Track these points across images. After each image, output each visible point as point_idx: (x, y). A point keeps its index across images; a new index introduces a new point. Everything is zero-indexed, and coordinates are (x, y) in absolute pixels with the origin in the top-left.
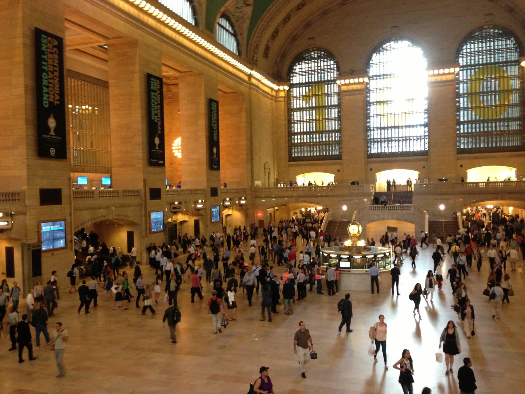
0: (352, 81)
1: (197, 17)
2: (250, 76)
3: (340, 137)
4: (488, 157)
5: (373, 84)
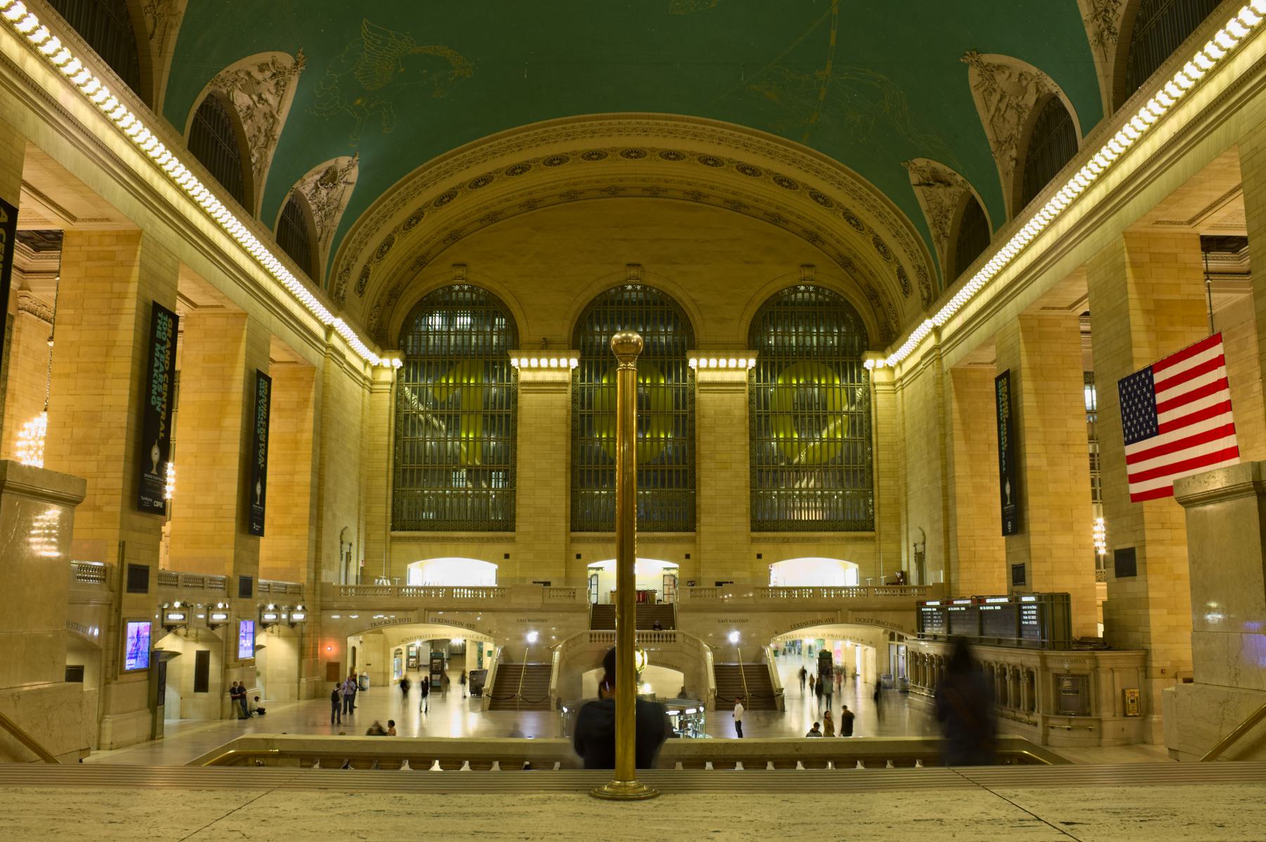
2: (329, 330)
4: (808, 540)
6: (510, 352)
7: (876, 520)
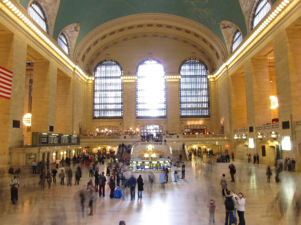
0: (129, 78)
1: (48, 30)
2: (74, 69)
3: (122, 107)
5: (139, 81)
7: (211, 115)
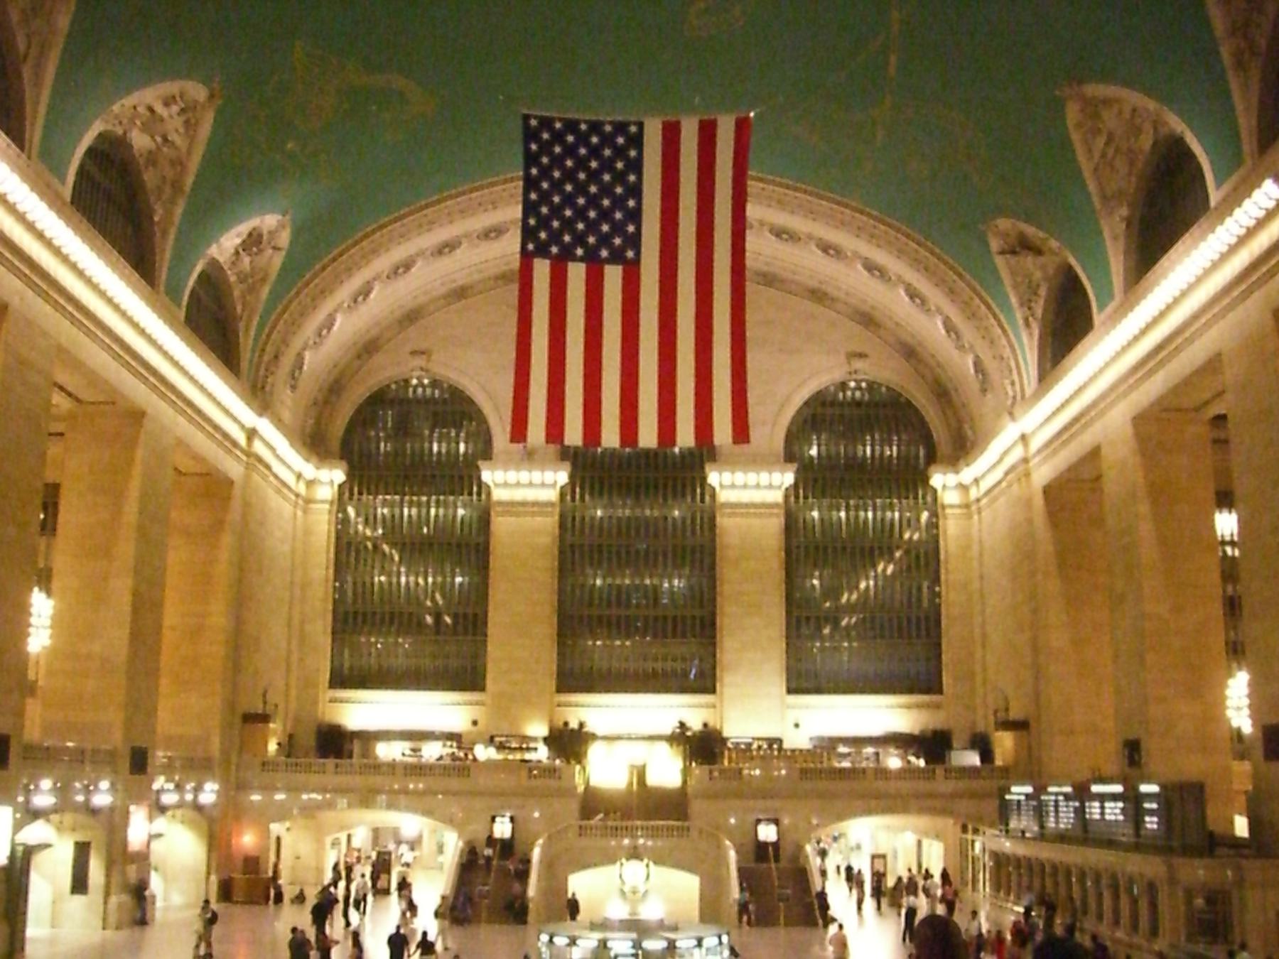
2: (252, 434)
6: (480, 463)
